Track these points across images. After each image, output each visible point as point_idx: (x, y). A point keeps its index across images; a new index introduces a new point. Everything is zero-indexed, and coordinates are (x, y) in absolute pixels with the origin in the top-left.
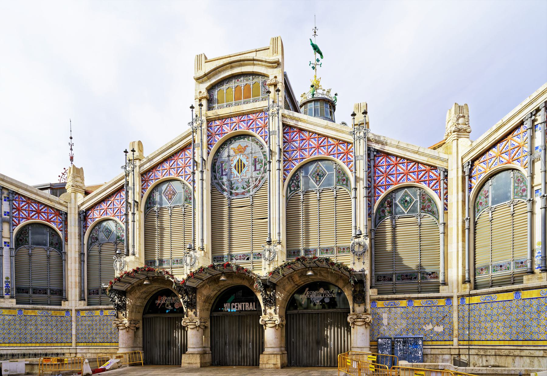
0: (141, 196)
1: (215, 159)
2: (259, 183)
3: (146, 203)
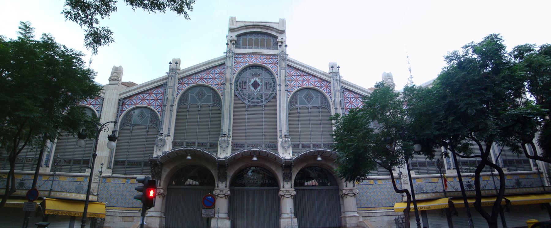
0: (177, 94)
1: (238, 78)
2: (269, 97)
3: (180, 100)
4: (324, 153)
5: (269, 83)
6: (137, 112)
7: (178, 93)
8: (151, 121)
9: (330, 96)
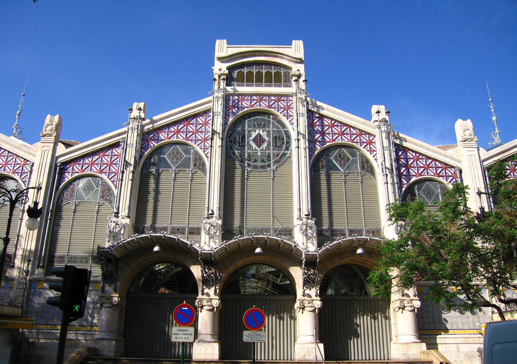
4: (367, 244)
5: (279, 137)
6: (82, 183)
7: (143, 155)
8: (102, 197)
9: (375, 158)
